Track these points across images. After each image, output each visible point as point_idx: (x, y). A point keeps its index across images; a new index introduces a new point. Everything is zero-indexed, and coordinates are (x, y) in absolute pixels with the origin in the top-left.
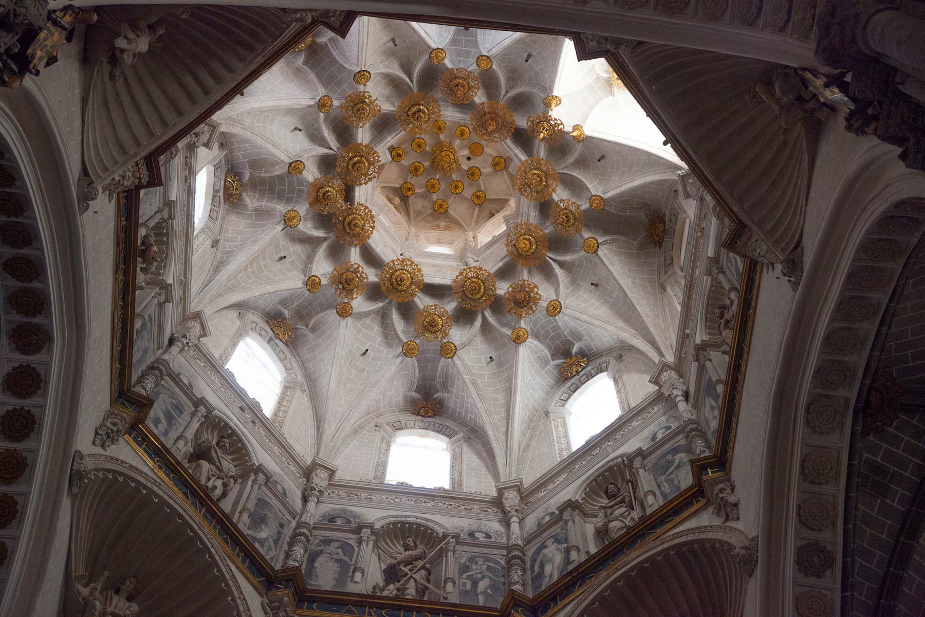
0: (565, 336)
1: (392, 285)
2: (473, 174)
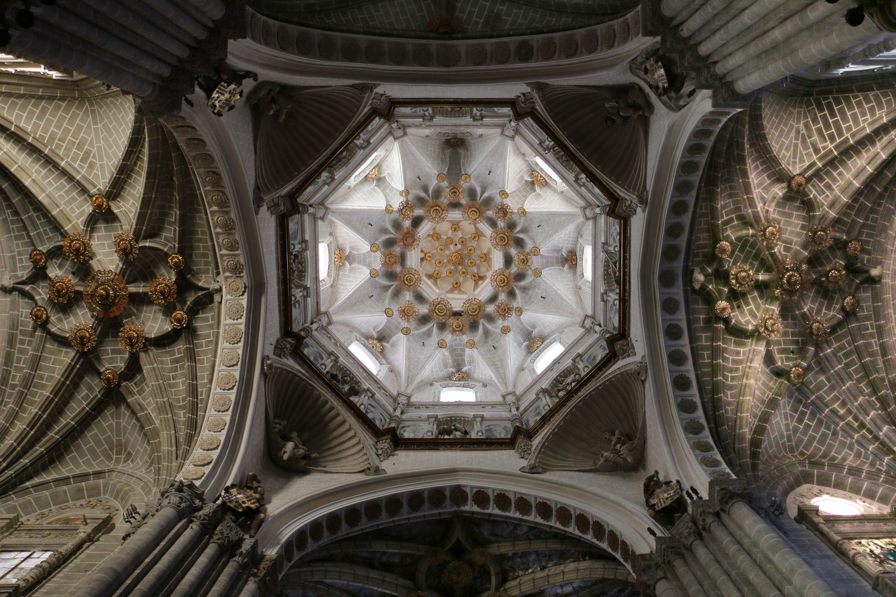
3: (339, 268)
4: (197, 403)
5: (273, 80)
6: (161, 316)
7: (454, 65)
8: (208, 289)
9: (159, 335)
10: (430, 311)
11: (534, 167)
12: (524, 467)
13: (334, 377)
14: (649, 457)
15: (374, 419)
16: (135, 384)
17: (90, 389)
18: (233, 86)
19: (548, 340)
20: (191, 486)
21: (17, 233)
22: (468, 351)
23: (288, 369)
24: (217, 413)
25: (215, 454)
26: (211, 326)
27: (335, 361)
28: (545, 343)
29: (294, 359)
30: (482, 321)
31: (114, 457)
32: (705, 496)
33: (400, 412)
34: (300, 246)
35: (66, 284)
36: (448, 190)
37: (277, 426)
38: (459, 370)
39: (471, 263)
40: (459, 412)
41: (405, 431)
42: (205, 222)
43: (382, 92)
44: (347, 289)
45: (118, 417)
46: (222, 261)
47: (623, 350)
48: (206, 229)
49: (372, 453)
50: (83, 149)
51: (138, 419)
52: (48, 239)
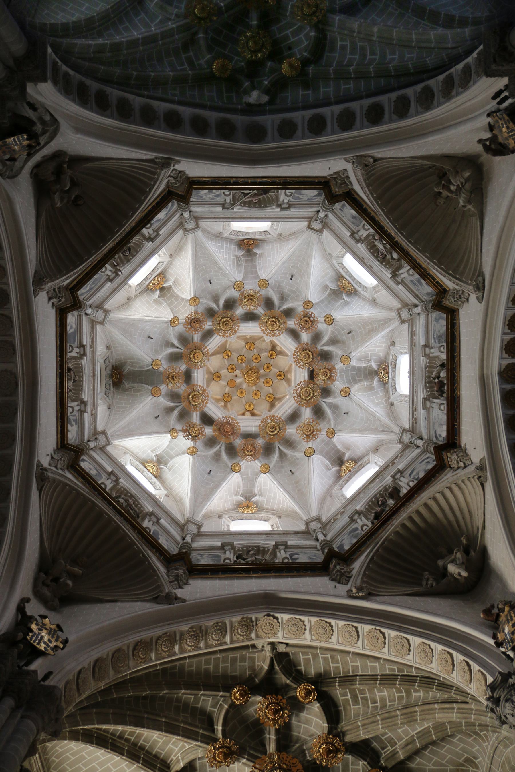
0: (164, 300)
1: (279, 321)
2: (233, 369)
3: (259, 508)
4: (403, 675)
5: (31, 580)
6: (304, 715)
7: (16, 378)
8: (272, 659)
9: (325, 718)
10: (308, 406)
11: (143, 287)
12: (477, 298)
13: (377, 516)
14: (464, 151)
15: (425, 471)
16: (383, 749)
18: (34, 627)
19: (341, 271)
20: (492, 687)
22: (354, 363)
23: (364, 568)
24: (411, 653)
25: (458, 657)
26: (315, 656)
27: (360, 515)
28: (344, 274)
29: (353, 561)
30: (319, 347)
32: (505, 81)
33: (420, 441)
34: (228, 552)
36: (170, 385)
37: (429, 582)
38: (376, 373)
39: (256, 359)
40: (420, 373)
41: (440, 436)
42: (195, 660)
43: (49, 458)
44: (283, 500)
46: (238, 641)
47: (341, 184)
48: (203, 659)
49: (461, 473)
51: (425, 747)
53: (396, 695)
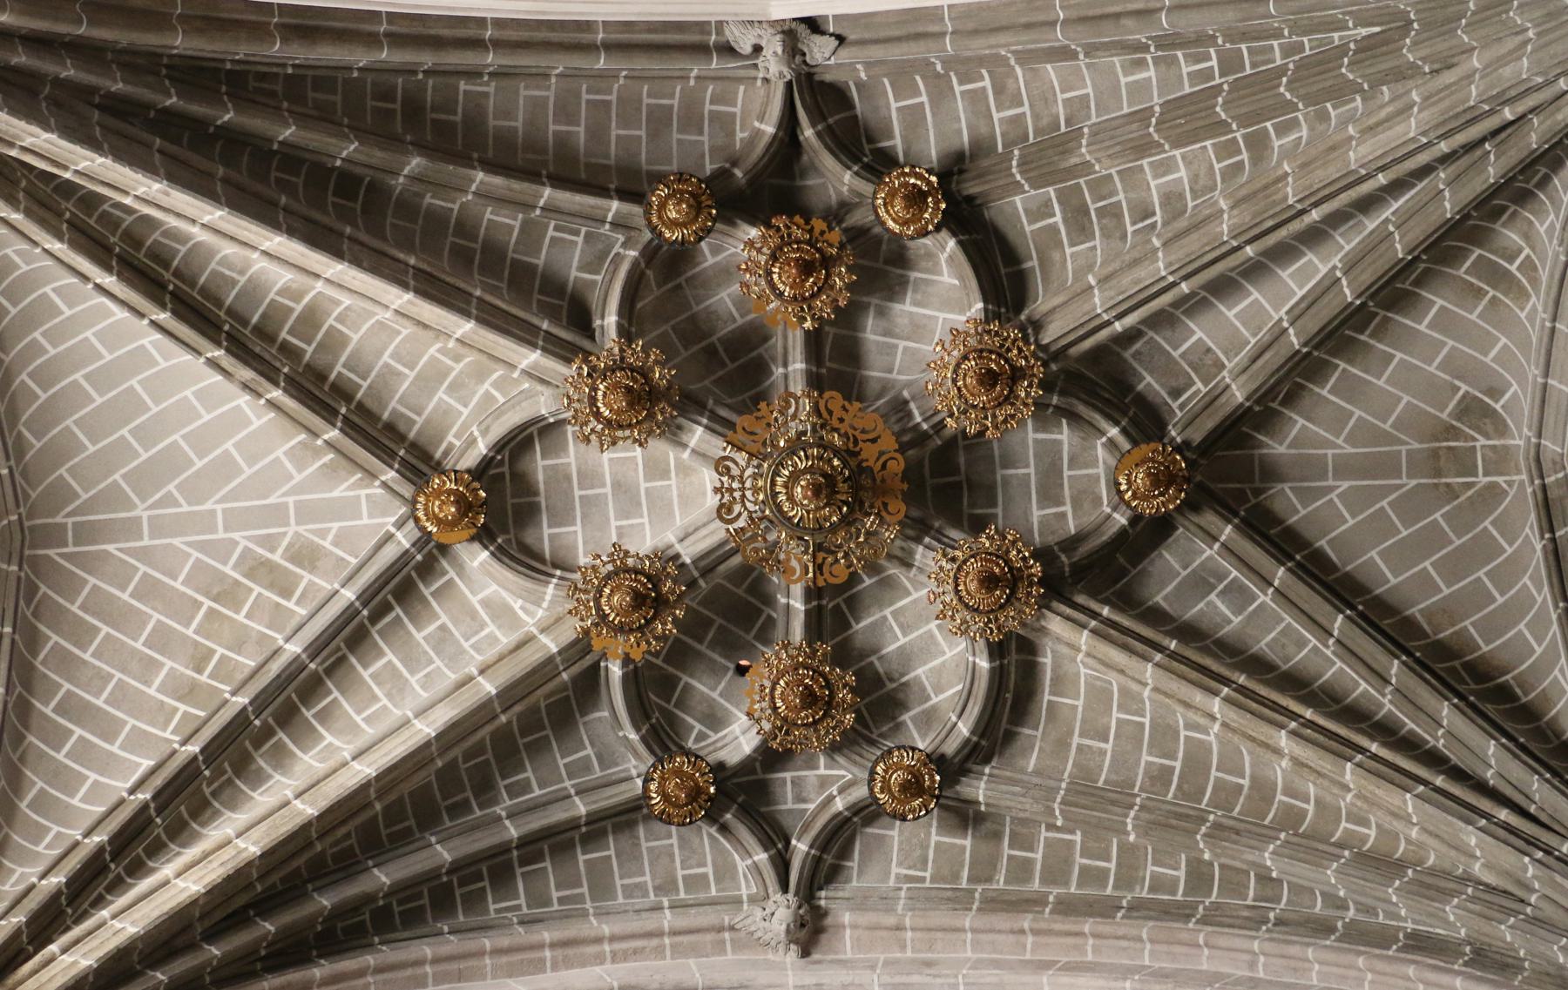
8: (789, 85)
16: (1176, 393)
17: (1202, 582)
21: (585, 889)
26: (940, 90)
31: (1483, 480)
35: (781, 674)
45: (1316, 468)
50: (237, 582)
52: (604, 764)
53: (1217, 166)
